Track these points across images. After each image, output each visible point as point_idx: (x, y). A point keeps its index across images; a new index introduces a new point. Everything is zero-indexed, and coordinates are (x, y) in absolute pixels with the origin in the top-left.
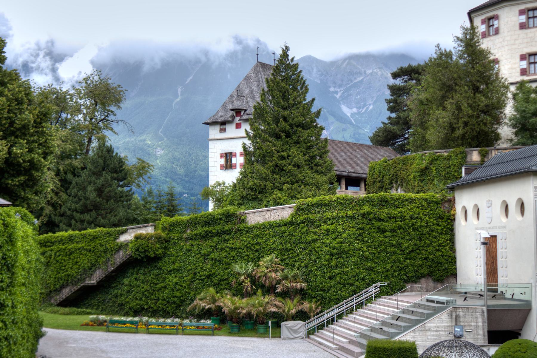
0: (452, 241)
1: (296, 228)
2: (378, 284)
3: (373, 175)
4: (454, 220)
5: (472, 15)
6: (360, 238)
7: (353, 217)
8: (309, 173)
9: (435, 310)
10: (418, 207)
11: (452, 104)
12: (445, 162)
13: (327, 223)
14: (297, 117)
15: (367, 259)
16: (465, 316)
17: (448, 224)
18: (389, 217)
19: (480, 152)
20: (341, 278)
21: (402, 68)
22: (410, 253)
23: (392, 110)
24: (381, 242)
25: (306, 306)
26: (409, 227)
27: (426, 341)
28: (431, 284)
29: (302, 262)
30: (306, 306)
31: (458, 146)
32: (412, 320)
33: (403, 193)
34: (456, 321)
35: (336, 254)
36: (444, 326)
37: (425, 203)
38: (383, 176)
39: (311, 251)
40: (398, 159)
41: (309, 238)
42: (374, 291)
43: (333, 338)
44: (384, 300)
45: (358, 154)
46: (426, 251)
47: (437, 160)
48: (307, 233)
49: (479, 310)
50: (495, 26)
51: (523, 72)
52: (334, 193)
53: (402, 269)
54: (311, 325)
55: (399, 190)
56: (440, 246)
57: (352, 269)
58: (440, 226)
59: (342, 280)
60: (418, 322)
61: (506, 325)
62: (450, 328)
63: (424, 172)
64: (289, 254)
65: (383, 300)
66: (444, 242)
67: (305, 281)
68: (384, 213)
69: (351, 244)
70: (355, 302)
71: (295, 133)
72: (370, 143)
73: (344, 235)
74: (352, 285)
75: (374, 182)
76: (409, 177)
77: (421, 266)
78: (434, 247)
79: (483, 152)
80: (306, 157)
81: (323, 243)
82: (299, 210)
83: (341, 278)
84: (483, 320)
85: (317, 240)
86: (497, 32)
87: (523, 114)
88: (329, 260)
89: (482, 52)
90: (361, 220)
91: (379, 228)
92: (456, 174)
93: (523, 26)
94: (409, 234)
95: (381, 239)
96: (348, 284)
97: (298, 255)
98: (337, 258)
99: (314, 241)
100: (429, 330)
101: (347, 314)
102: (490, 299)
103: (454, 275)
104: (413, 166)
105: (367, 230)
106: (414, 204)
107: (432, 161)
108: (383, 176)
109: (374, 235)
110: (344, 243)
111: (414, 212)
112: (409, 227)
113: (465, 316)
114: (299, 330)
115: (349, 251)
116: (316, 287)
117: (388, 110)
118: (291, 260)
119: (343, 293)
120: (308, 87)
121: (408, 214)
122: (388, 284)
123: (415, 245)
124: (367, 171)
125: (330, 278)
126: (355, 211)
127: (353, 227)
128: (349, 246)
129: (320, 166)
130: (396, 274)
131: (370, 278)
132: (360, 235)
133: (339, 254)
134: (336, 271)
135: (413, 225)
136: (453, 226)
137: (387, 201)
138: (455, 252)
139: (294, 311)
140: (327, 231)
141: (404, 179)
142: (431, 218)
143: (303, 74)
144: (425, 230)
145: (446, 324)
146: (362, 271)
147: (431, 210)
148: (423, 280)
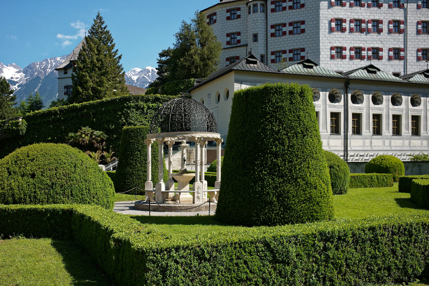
50: (214, 19)
86: (215, 21)
93: (228, 18)
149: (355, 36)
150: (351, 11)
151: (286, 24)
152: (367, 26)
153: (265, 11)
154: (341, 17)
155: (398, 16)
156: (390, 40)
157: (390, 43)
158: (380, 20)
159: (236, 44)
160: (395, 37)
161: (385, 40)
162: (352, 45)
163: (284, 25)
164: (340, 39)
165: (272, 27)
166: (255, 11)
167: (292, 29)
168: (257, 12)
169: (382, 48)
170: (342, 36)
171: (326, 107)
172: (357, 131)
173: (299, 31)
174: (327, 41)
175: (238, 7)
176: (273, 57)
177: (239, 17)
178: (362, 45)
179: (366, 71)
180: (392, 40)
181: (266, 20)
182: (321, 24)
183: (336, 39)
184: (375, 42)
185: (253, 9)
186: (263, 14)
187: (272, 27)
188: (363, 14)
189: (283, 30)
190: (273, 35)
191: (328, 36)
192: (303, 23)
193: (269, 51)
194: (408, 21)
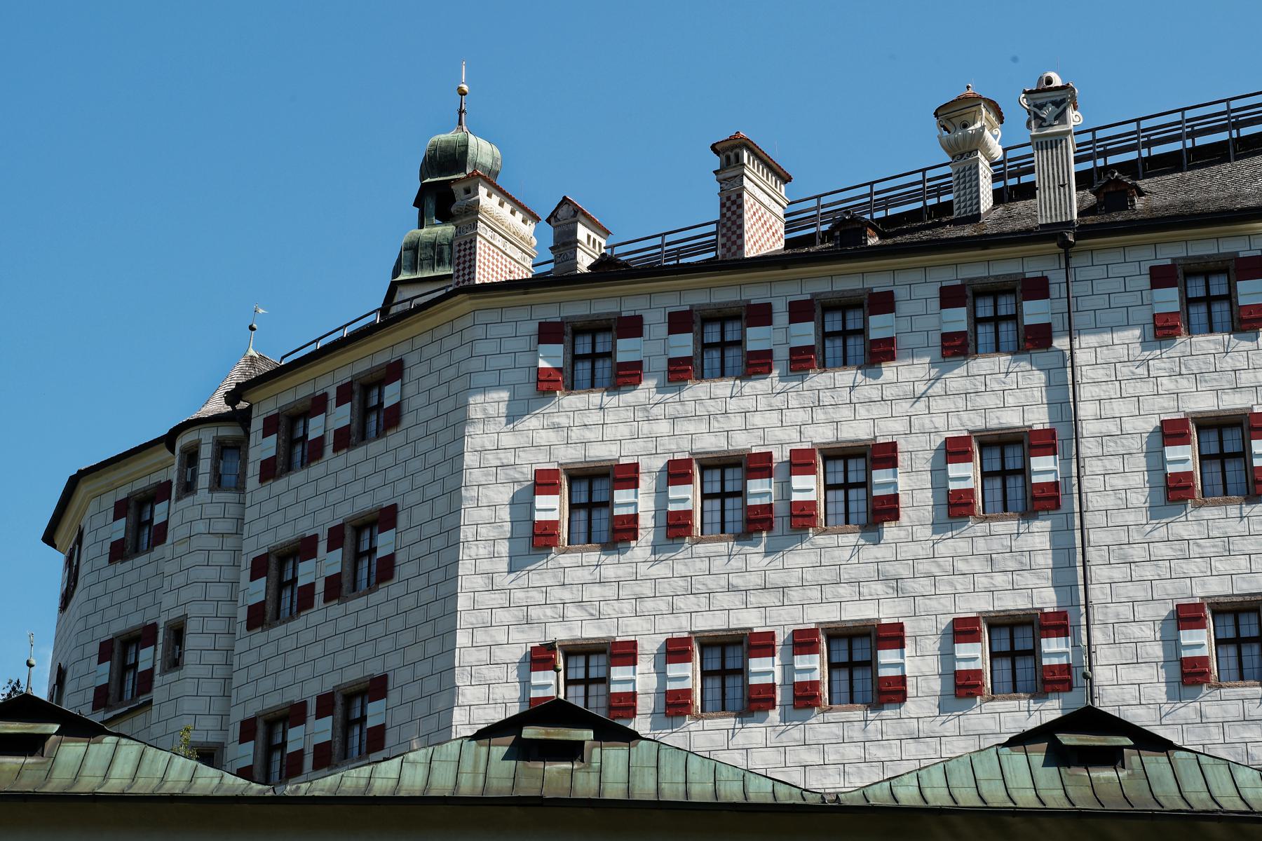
149: (703, 565)
150: (671, 410)
152: (786, 488)
154: (602, 452)
155: (1010, 401)
156: (961, 566)
157: (961, 584)
158: (881, 440)
160: (996, 545)
161: (923, 567)
162: (679, 626)
164: (596, 592)
169: (900, 627)
170: (609, 572)
174: (502, 616)
178: (752, 620)
180: (977, 565)
182: (470, 515)
183: (566, 595)
184: (844, 591)
188: (757, 420)
191: (504, 580)
194: (1088, 428)
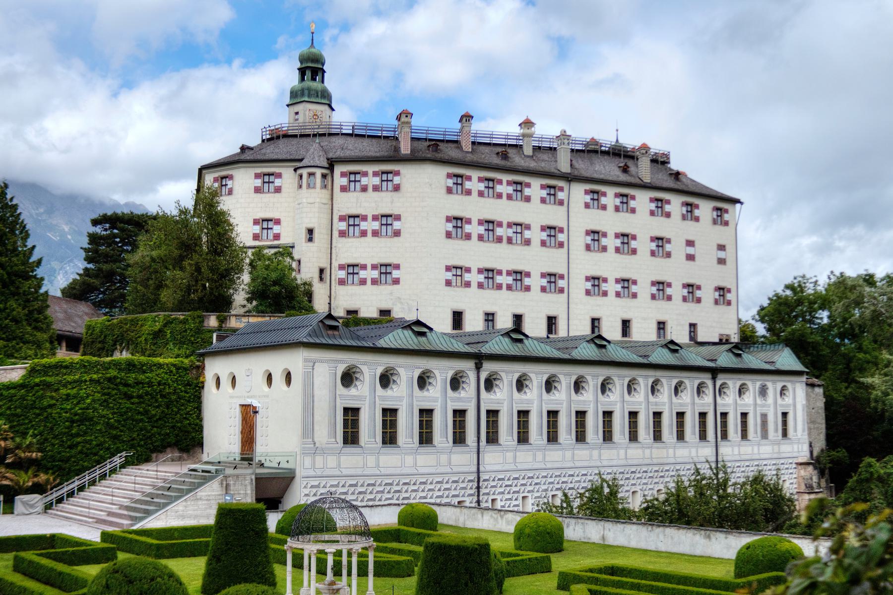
0: (199, 409)
1: (28, 391)
2: (124, 454)
3: (92, 334)
4: (203, 387)
5: (204, 172)
6: (105, 404)
7: (98, 382)
8: (29, 329)
9: (204, 479)
10: (166, 373)
11: (190, 265)
12: (181, 326)
13: (66, 387)
14: (16, 265)
15: (112, 427)
16: (234, 484)
17: (196, 391)
18: (135, 383)
19: (218, 318)
20: (84, 447)
21: (106, 214)
22: (157, 421)
23: (89, 260)
24: (127, 408)
25: (43, 477)
26: (157, 393)
27: (197, 510)
28: (177, 454)
29: (35, 429)
30: (43, 477)
31: (195, 309)
32: (183, 489)
33: (130, 356)
34: (226, 490)
35: (78, 421)
36: (215, 495)
37: (174, 369)
38: (105, 337)
39: (46, 417)
40: (125, 319)
41: (45, 403)
42: (119, 461)
43: (89, 513)
44: (129, 470)
45: (57, 308)
46: (174, 419)
47: (172, 323)
48: (42, 397)
49: (248, 478)
50: (229, 187)
51: (256, 237)
52: (54, 354)
53: (150, 438)
54: (50, 498)
55: (124, 353)
56: (188, 413)
57: (96, 437)
58: (188, 393)
59: (84, 449)
60: (190, 491)
61: (271, 493)
62: (221, 497)
63: (157, 335)
64: (19, 421)
65: (130, 470)
66: (191, 410)
67: (39, 450)
68: (132, 377)
69: (95, 410)
70: (98, 472)
71: (13, 282)
72: (59, 294)
73: (88, 401)
74: (95, 454)
75: (93, 342)
76: (139, 339)
77: (168, 434)
78: (181, 415)
79: (222, 318)
80: (26, 311)
81: (62, 409)
82: (32, 371)
83: (84, 447)
84: (252, 488)
85: (54, 405)
86: (230, 192)
87: (264, 281)
88: (70, 428)
89: (223, 213)
90: (106, 384)
91: (125, 394)
92: (193, 339)
93: (257, 190)
94: (157, 401)
95: (127, 405)
96: (91, 453)
97: (31, 422)
98: (79, 426)
99: (51, 406)
100: (201, 499)
101: (89, 486)
102: (257, 468)
103: (201, 444)
104: (144, 328)
105: (113, 396)
106: (162, 370)
107: (166, 323)
108: (105, 337)
109: (120, 401)
110: (87, 409)
111: (163, 378)
112: (157, 393)
113: (234, 484)
114: (36, 505)
115: (93, 418)
116: (52, 456)
117: (85, 260)
118: (22, 428)
119: (86, 464)
120: (29, 232)
121: (156, 379)
122: (134, 454)
123: (163, 412)
124: (83, 331)
125: (70, 447)
126: (100, 375)
127: (98, 392)
128: (93, 412)
129: (40, 321)
130: (142, 443)
131: (115, 447)
132: (105, 401)
133: (82, 421)
134: (79, 439)
135: (160, 391)
136: (200, 393)
137: (134, 366)
138: (201, 420)
139: (30, 484)
140: (68, 395)
141: (132, 341)
142: (179, 385)
143: (22, 217)
144: (174, 397)
145: (217, 493)
146: (107, 440)
147: (180, 377)
148: (169, 450)
151: (366, 216)
153: (330, 187)
159: (271, 241)
163: (364, 218)
165: (342, 219)
166: (312, 185)
167: (377, 228)
168: (314, 188)
171: (446, 401)
172: (493, 438)
173: (389, 233)
175: (277, 170)
176: (342, 274)
177: (278, 190)
179: (507, 340)
181: (330, 203)
185: (307, 181)
186: (324, 191)
187: (342, 219)
189: (362, 228)
190: (342, 234)
192: (398, 218)
193: (335, 264)
